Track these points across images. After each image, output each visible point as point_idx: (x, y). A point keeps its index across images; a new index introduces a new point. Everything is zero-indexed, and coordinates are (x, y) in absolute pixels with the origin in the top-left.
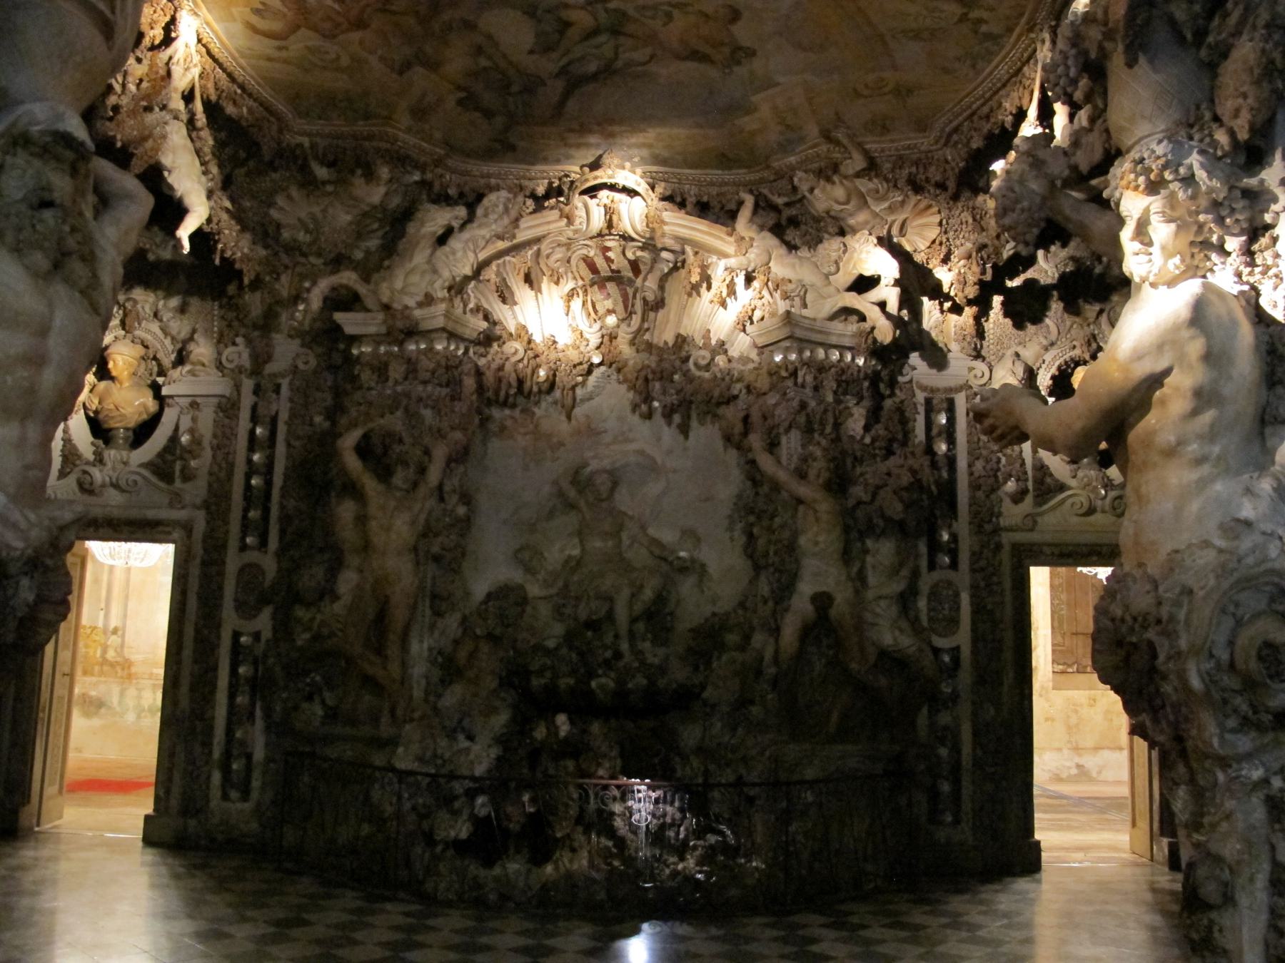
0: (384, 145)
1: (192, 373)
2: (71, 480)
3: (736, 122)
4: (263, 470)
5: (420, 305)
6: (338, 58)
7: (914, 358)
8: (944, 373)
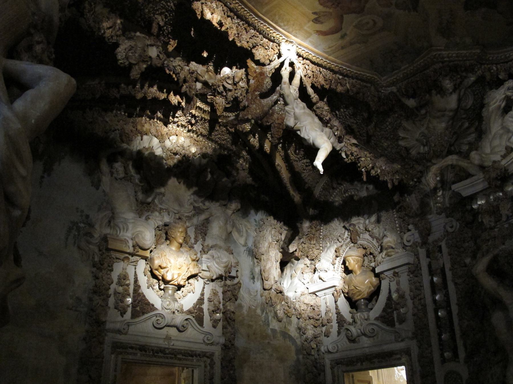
0: (437, 66)
1: (387, 255)
5: (504, 157)
6: (375, 23)
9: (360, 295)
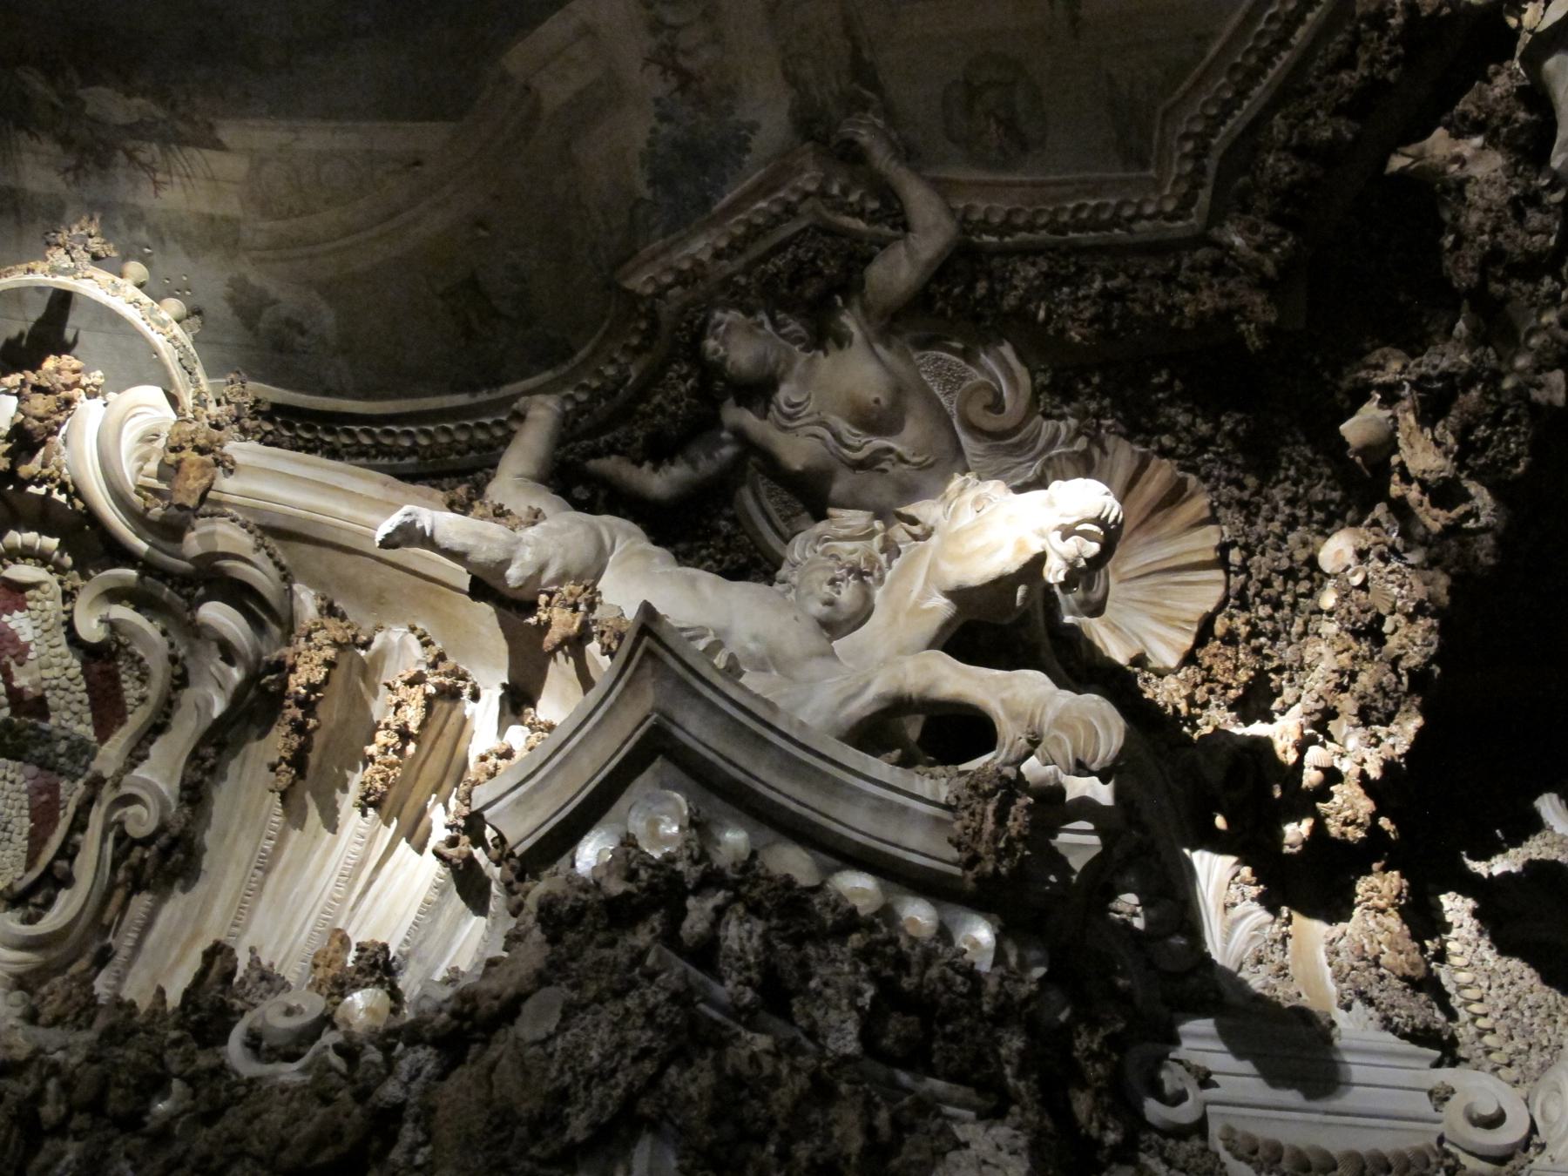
3: (516, 60)
7: (1199, 1040)
8: (1335, 1104)
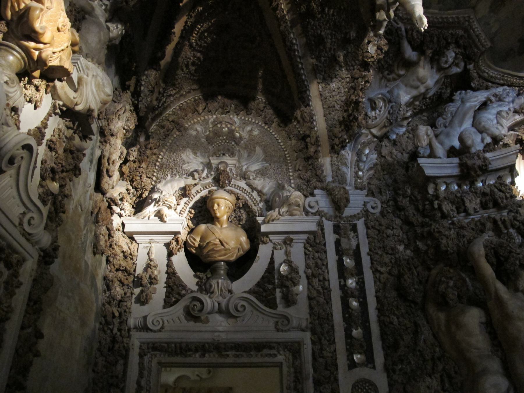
0: (461, 32)
2: (179, 309)
4: (357, 293)
9: (225, 255)
